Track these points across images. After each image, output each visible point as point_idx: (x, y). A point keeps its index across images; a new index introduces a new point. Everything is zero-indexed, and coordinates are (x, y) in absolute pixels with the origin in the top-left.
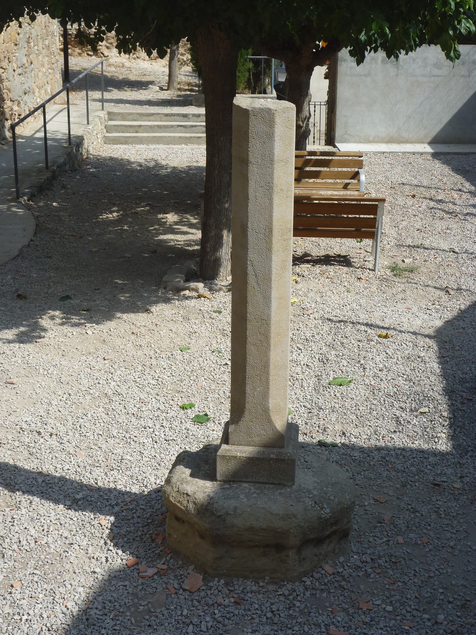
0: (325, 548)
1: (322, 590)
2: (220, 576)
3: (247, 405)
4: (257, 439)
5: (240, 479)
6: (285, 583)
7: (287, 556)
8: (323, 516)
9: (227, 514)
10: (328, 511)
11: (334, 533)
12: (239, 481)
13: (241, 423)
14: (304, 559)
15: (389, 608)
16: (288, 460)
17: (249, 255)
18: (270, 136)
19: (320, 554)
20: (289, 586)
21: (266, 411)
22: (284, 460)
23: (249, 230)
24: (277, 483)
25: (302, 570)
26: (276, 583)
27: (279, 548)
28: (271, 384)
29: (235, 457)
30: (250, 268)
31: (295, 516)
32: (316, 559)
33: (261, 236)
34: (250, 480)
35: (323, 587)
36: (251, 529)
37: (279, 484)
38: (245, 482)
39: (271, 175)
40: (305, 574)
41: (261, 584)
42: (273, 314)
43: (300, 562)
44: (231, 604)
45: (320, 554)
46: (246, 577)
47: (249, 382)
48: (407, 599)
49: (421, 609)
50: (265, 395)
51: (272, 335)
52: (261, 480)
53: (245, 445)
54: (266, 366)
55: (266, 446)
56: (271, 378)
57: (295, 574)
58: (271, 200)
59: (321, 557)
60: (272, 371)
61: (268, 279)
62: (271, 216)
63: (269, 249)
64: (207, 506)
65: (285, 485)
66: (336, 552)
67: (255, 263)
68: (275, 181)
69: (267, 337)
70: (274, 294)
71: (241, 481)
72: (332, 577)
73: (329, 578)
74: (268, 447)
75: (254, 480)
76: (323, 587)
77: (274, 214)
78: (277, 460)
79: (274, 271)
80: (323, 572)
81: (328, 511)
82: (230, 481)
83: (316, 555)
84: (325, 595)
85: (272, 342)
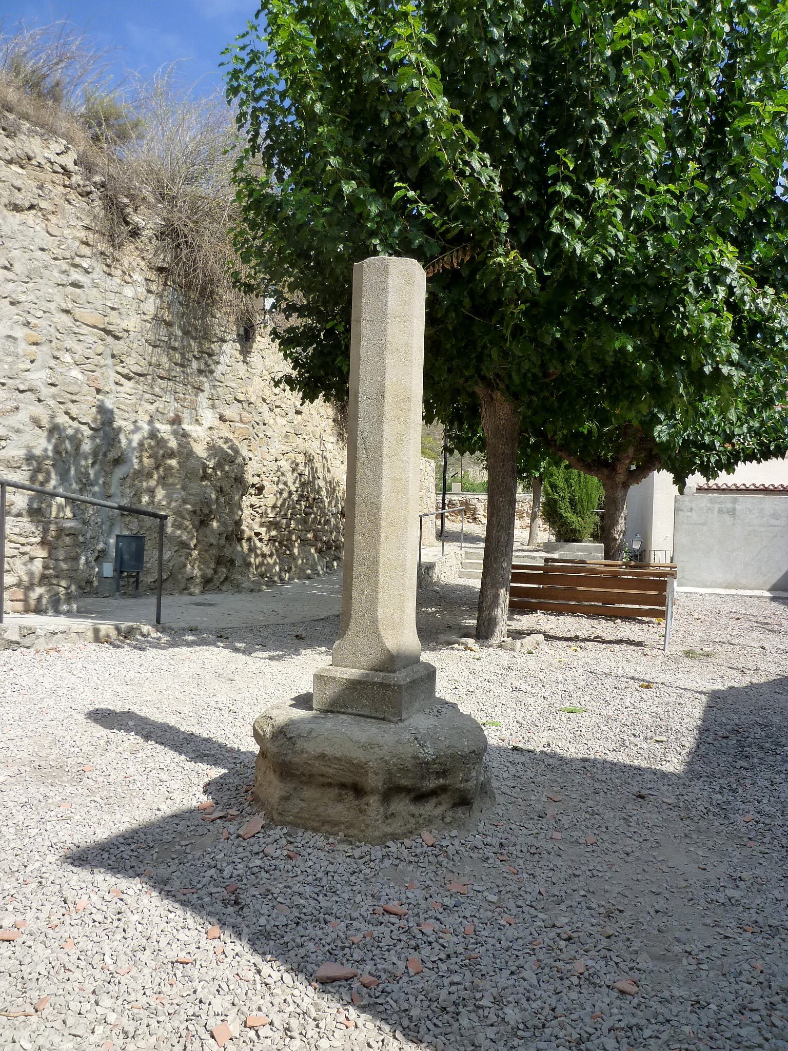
0: (428, 809)
1: (410, 862)
2: (284, 824)
3: (353, 613)
4: (363, 659)
5: (338, 709)
6: (362, 844)
7: (367, 804)
8: (420, 755)
9: (300, 736)
10: (431, 751)
11: (443, 789)
12: (337, 712)
13: (346, 636)
14: (393, 814)
15: (493, 898)
16: (394, 685)
17: (360, 425)
18: (384, 288)
19: (420, 816)
20: (365, 848)
21: (374, 621)
22: (389, 685)
23: (360, 395)
24: (381, 716)
25: (388, 830)
26: (351, 843)
27: (359, 791)
28: (380, 586)
29: (334, 678)
30: (360, 441)
31: (380, 747)
32: (413, 820)
33: (373, 402)
34: (350, 710)
35: (412, 859)
36: (322, 757)
37: (383, 719)
38: (344, 713)
39: (384, 331)
40: (394, 837)
41: (331, 840)
42: (384, 498)
43: (386, 818)
44: (282, 857)
45: (420, 816)
46: (315, 830)
47: (356, 583)
48: (526, 892)
49: (539, 907)
50: (373, 601)
51: (383, 523)
52: (362, 712)
53: (349, 667)
54: (375, 562)
55: (375, 669)
56: (380, 578)
57: (377, 834)
58: (383, 358)
59: (421, 821)
60: (382, 571)
61: (378, 452)
62: (383, 378)
63: (381, 417)
64: (283, 727)
65: (390, 721)
66: (448, 820)
67: (365, 434)
68: (389, 337)
69: (376, 525)
70: (386, 471)
71: (340, 712)
72: (430, 849)
73: (424, 850)
74: (376, 670)
75: (354, 711)
76: (412, 859)
77: (387, 375)
78: (381, 684)
79: (386, 444)
80: (420, 840)
81: (431, 751)
82: (327, 711)
83: (413, 816)
84: (411, 868)
85: (383, 531)
